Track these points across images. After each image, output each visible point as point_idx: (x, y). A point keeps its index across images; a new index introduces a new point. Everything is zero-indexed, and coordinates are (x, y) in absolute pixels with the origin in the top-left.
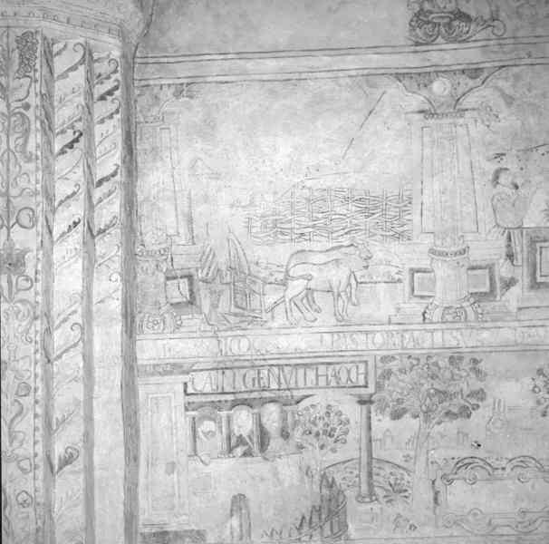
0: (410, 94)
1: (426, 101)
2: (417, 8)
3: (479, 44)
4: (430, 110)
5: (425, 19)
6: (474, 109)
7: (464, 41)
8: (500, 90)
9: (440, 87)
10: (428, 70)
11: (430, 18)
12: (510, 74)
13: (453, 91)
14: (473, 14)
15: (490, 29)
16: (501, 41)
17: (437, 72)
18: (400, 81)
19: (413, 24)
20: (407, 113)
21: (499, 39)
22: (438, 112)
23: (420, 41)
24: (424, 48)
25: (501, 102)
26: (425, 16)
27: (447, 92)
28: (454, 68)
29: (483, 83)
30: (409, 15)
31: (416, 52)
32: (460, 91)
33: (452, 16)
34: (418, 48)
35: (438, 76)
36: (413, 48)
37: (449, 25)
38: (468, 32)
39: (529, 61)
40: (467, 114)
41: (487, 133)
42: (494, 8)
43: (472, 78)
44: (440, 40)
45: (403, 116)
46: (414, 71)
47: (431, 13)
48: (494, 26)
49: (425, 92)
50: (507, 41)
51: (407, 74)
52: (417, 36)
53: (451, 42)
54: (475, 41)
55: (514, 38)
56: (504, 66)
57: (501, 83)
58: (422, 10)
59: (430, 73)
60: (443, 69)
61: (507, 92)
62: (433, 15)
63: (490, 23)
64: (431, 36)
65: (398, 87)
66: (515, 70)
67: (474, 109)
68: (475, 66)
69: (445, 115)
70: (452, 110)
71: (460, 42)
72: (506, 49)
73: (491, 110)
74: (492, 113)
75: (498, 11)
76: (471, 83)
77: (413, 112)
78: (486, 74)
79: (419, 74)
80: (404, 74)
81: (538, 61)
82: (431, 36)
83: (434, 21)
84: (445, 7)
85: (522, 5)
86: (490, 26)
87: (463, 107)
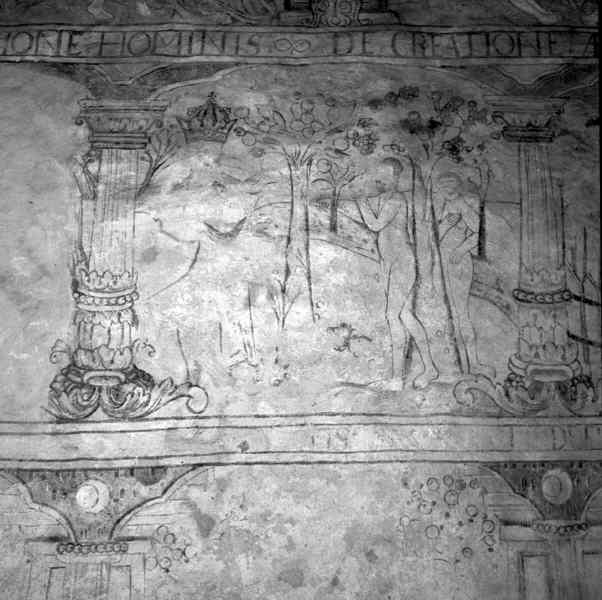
0: (37, 507)
1: (64, 521)
2: (66, 361)
3: (164, 424)
4: (69, 537)
5: (79, 380)
6: (144, 539)
7: (141, 418)
8: (192, 505)
9: (90, 498)
10: (71, 465)
11: (86, 378)
12: (211, 479)
13: (113, 504)
14: (158, 375)
15: (185, 399)
16: (200, 423)
17: (85, 470)
18: (24, 483)
19: (57, 386)
20: (28, 541)
21: (196, 417)
22: (84, 540)
23: (67, 415)
24: (69, 427)
25: (192, 527)
26: (79, 375)
27: (99, 507)
28: (117, 464)
29: (165, 491)
30: (50, 372)
31: (55, 434)
32: (125, 502)
33: (123, 377)
34: (60, 427)
35: (87, 478)
36: (49, 428)
37: (116, 392)
38: (147, 404)
39: (243, 458)
40: (133, 547)
41: (163, 584)
42: (192, 367)
43: (146, 483)
44: (99, 414)
45: (20, 545)
46: (56, 466)
47: (91, 370)
48: (189, 396)
49: (62, 505)
50: (207, 423)
51: (37, 470)
52: (60, 407)
53: (118, 420)
54: (156, 419)
55: (220, 417)
56: (201, 465)
57: (195, 494)
58: (74, 364)
59: (74, 470)
60: (97, 466)
61: (204, 510)
62: (92, 374)
63: (183, 390)
64: (85, 408)
65: (18, 493)
66: (220, 472)
67: (144, 539)
68: (153, 463)
69: (93, 547)
70: (106, 538)
71: (132, 420)
72: (207, 435)
73: (174, 541)
74: (174, 547)
75: (199, 371)
76: (144, 491)
77: (39, 539)
78: (169, 477)
79: (57, 473)
80: (32, 471)
81: (259, 458)
82: (85, 408)
83: (92, 382)
84: (112, 362)
85: (237, 365)
86: (182, 396)
87: (124, 534)
